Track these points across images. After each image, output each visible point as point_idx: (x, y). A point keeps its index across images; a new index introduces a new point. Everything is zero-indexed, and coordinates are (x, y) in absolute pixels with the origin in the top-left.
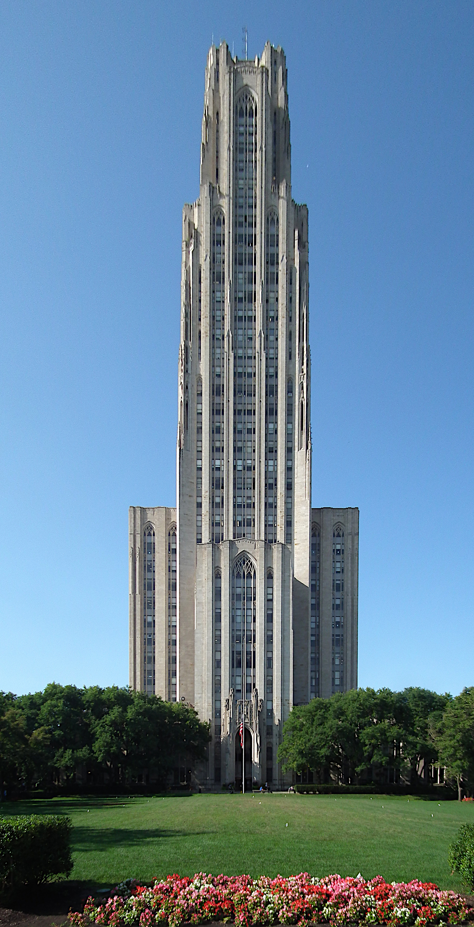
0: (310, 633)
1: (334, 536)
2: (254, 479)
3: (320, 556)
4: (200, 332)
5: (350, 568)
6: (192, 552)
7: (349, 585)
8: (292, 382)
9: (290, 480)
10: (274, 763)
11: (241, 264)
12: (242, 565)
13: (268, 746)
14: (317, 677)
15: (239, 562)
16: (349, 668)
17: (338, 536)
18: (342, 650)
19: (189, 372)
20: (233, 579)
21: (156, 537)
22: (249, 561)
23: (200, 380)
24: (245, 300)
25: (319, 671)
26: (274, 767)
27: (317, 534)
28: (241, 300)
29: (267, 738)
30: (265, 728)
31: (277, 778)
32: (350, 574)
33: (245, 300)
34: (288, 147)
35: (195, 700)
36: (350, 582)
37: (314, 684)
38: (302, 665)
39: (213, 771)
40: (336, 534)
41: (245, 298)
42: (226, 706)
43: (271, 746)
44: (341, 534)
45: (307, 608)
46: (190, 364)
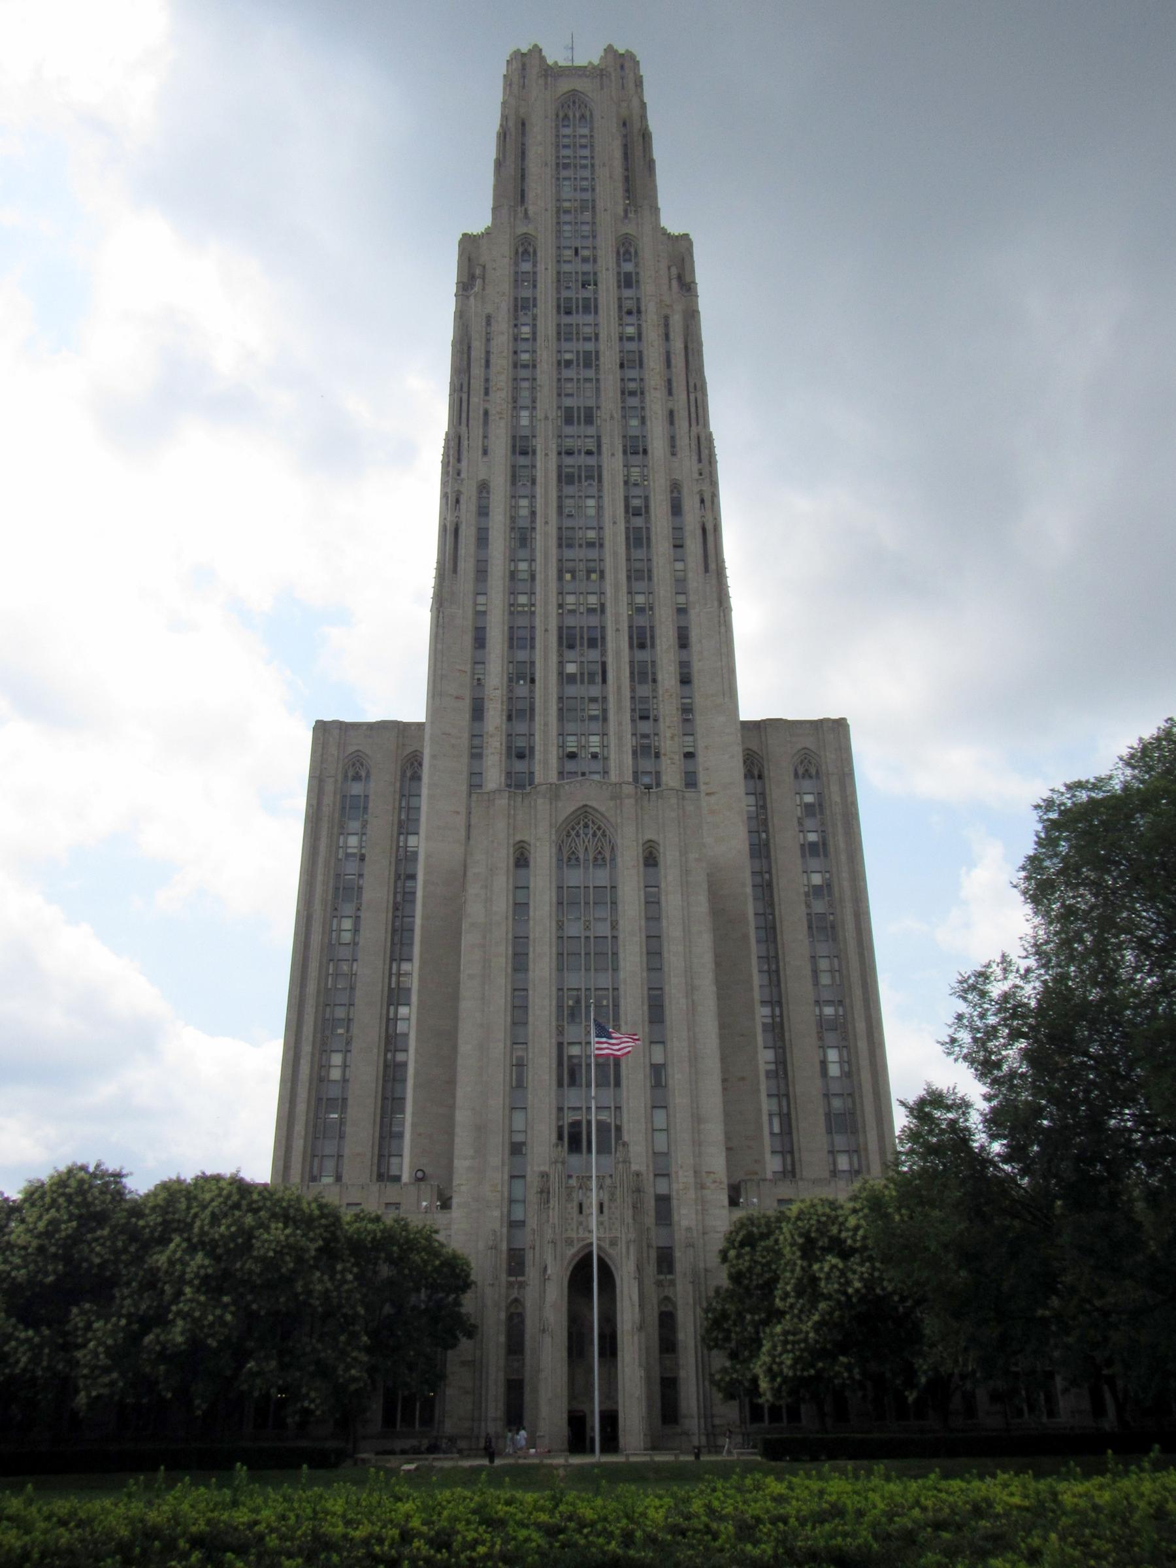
0: (757, 995)
1: (796, 775)
2: (604, 664)
3: (766, 819)
4: (486, 413)
5: (842, 845)
6: (458, 813)
7: (846, 884)
8: (679, 492)
9: (686, 670)
10: (681, 1362)
11: (568, 313)
12: (582, 835)
13: (664, 1309)
14: (785, 1110)
15: (573, 829)
16: (867, 1087)
17: (807, 775)
18: (844, 1039)
19: (463, 475)
20: (560, 867)
21: (372, 784)
22: (599, 828)
23: (484, 487)
24: (578, 365)
25: (787, 1096)
26: (682, 1374)
27: (756, 773)
28: (568, 363)
29: (659, 1284)
30: (653, 1254)
31: (694, 1410)
32: (843, 857)
33: (578, 365)
34: (650, 165)
35: (455, 1176)
36: (845, 875)
37: (776, 1130)
38: (743, 1079)
39: (502, 1390)
40: (801, 771)
41: (578, 359)
42: (542, 1192)
43: (670, 1308)
44: (813, 771)
45: (745, 937)
46: (464, 463)
